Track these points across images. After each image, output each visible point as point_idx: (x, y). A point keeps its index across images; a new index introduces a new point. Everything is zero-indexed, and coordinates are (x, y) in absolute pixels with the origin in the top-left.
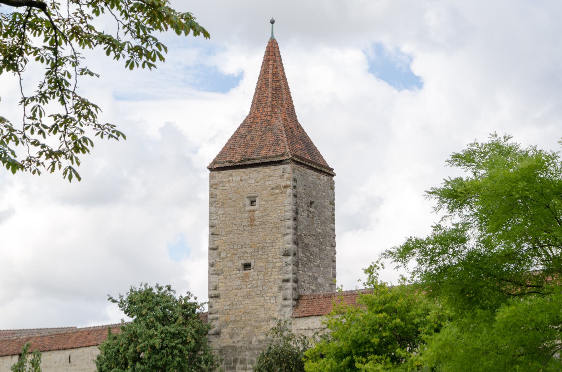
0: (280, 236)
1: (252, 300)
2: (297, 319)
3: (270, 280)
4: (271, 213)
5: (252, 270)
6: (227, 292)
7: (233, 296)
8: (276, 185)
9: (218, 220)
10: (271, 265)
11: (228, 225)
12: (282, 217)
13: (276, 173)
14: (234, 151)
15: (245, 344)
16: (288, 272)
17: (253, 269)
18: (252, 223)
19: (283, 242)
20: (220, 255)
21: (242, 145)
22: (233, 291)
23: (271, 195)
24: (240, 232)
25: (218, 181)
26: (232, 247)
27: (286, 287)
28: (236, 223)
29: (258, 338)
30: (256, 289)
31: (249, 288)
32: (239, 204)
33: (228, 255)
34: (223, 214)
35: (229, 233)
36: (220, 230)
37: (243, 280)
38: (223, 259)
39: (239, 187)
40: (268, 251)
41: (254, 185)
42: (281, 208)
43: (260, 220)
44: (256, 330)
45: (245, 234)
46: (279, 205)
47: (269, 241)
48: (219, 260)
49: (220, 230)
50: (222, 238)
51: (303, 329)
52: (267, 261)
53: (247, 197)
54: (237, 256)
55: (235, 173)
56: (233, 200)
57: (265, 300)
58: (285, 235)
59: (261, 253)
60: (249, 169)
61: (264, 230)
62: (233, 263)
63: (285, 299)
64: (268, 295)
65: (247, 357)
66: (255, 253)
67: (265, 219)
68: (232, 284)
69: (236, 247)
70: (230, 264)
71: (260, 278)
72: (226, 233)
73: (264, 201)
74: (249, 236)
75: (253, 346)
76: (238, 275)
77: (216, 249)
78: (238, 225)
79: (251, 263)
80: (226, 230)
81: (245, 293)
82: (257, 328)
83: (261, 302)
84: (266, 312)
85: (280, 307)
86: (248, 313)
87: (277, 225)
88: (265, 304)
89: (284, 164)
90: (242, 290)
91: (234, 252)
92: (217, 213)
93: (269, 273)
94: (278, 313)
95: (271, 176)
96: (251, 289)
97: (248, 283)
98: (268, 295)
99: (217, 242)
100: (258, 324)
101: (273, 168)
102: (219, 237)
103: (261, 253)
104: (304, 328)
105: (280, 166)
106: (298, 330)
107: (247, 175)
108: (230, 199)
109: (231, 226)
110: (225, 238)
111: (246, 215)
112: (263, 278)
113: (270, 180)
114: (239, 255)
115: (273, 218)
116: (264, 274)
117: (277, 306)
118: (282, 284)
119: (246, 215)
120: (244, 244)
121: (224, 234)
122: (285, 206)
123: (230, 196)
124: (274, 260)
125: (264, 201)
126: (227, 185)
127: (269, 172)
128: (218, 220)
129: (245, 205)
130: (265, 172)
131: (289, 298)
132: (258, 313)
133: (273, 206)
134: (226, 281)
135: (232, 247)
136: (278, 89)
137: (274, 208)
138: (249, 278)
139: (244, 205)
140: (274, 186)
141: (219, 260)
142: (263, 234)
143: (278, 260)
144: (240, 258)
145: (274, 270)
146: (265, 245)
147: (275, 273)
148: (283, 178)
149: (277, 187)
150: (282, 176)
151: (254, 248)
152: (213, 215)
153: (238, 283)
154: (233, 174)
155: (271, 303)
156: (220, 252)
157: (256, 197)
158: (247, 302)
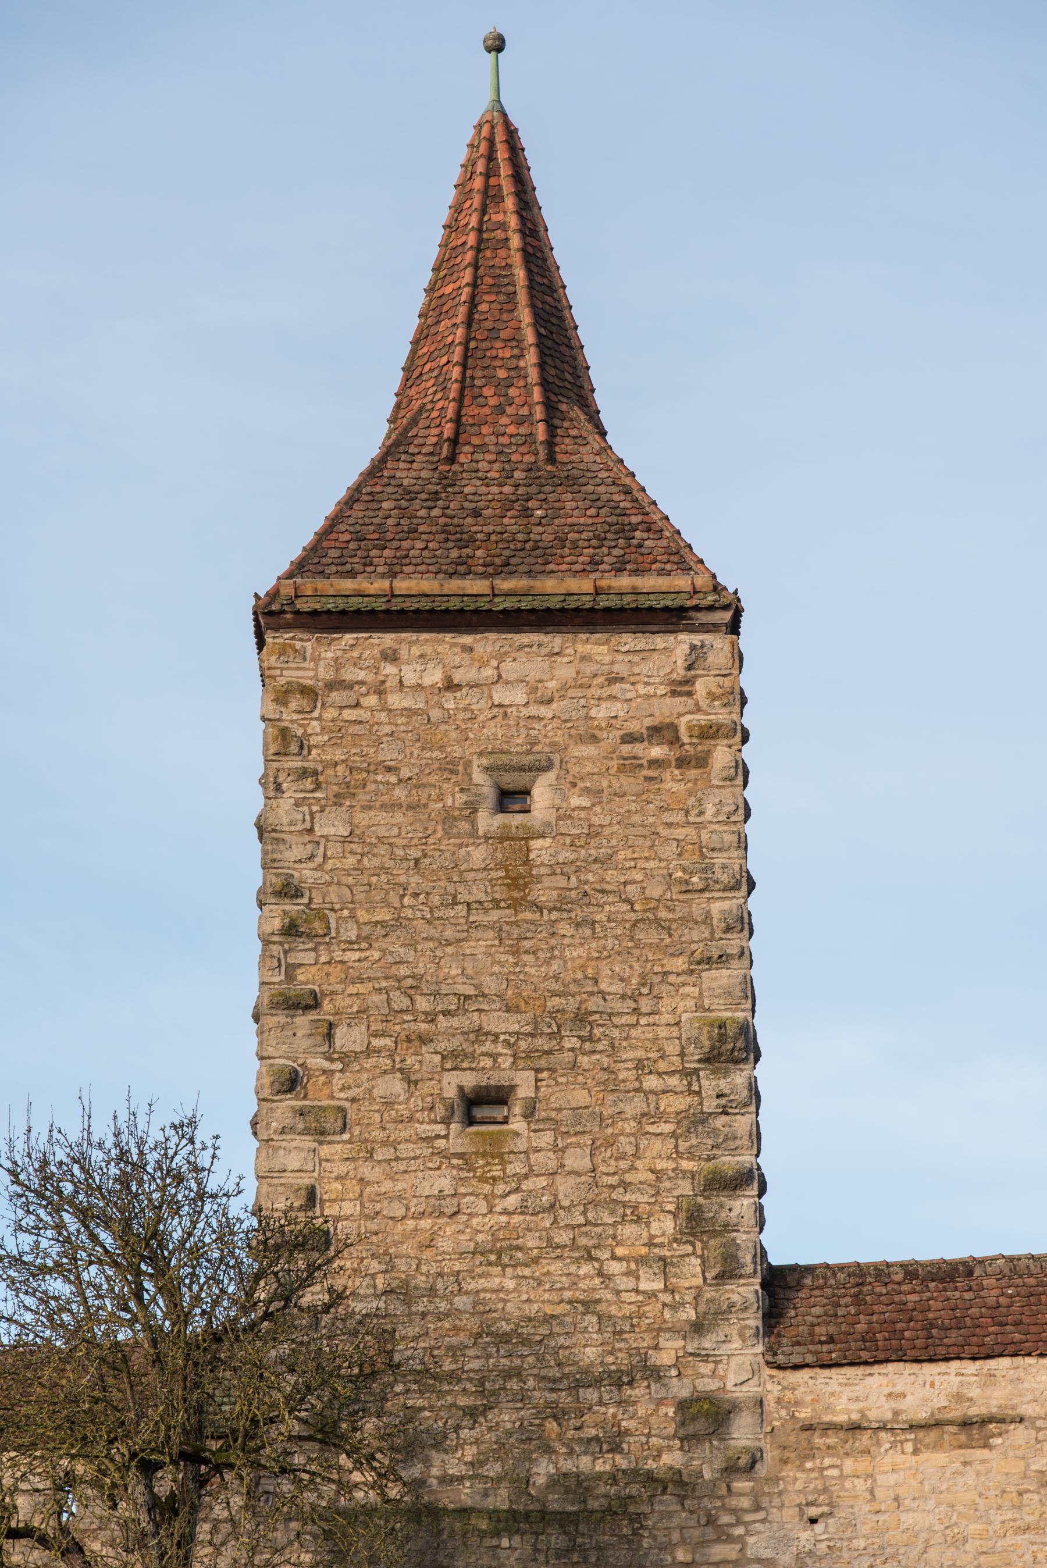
0: (680, 963)
1: (520, 1271)
3: (628, 1177)
7: (408, 1248)
8: (648, 722)
9: (320, 867)
10: (636, 1105)
11: (378, 897)
13: (644, 668)
14: (387, 553)
15: (486, 1494)
16: (732, 1144)
18: (516, 894)
20: (329, 1036)
21: (421, 529)
22: (410, 1224)
23: (622, 769)
25: (315, 677)
26: (400, 1001)
28: (426, 886)
31: (505, 1212)
32: (441, 798)
33: (377, 1043)
34: (344, 840)
35: (379, 931)
38: (347, 1058)
39: (435, 714)
40: (616, 1033)
41: (525, 712)
42: (679, 833)
43: (562, 882)
44: (551, 1426)
45: (480, 944)
46: (667, 817)
47: (617, 988)
48: (326, 1065)
49: (332, 917)
50: (338, 955)
52: (611, 1084)
53: (487, 769)
54: (431, 1047)
55: (416, 651)
56: (405, 773)
57: (600, 1274)
58: (709, 960)
59: (575, 1042)
60: (492, 636)
61: (588, 932)
62: (411, 1083)
64: (620, 1251)
67: (590, 877)
68: (400, 1186)
69: (423, 1004)
70: (395, 1086)
72: (366, 930)
73: (587, 790)
74: (503, 958)
76: (441, 1143)
77: (307, 1008)
78: (436, 900)
79: (512, 1088)
80: (363, 916)
81: (480, 1238)
82: (555, 1417)
86: (504, 1338)
87: (663, 914)
89: (693, 629)
92: (311, 830)
93: (625, 1145)
95: (622, 680)
96: (516, 1219)
97: (500, 1188)
100: (565, 1399)
101: (629, 641)
103: (575, 1042)
105: (671, 638)
108: (389, 769)
109: (394, 899)
110: (356, 955)
111: (478, 855)
113: (612, 697)
114: (442, 1045)
115: (639, 876)
119: (478, 855)
120: (471, 991)
121: (353, 935)
122: (699, 826)
123: (388, 754)
124: (651, 1082)
125: (587, 790)
127: (607, 659)
128: (320, 867)
132: (561, 1340)
133: (637, 819)
134: (366, 1170)
136: (554, 320)
137: (640, 831)
138: (503, 1163)
141: (326, 1065)
143: (674, 1081)
144: (453, 1059)
147: (657, 1145)
148: (690, 694)
150: (682, 683)
151: (529, 1016)
153: (444, 1182)
154: (404, 653)
155: (637, 1291)
156: (331, 1026)
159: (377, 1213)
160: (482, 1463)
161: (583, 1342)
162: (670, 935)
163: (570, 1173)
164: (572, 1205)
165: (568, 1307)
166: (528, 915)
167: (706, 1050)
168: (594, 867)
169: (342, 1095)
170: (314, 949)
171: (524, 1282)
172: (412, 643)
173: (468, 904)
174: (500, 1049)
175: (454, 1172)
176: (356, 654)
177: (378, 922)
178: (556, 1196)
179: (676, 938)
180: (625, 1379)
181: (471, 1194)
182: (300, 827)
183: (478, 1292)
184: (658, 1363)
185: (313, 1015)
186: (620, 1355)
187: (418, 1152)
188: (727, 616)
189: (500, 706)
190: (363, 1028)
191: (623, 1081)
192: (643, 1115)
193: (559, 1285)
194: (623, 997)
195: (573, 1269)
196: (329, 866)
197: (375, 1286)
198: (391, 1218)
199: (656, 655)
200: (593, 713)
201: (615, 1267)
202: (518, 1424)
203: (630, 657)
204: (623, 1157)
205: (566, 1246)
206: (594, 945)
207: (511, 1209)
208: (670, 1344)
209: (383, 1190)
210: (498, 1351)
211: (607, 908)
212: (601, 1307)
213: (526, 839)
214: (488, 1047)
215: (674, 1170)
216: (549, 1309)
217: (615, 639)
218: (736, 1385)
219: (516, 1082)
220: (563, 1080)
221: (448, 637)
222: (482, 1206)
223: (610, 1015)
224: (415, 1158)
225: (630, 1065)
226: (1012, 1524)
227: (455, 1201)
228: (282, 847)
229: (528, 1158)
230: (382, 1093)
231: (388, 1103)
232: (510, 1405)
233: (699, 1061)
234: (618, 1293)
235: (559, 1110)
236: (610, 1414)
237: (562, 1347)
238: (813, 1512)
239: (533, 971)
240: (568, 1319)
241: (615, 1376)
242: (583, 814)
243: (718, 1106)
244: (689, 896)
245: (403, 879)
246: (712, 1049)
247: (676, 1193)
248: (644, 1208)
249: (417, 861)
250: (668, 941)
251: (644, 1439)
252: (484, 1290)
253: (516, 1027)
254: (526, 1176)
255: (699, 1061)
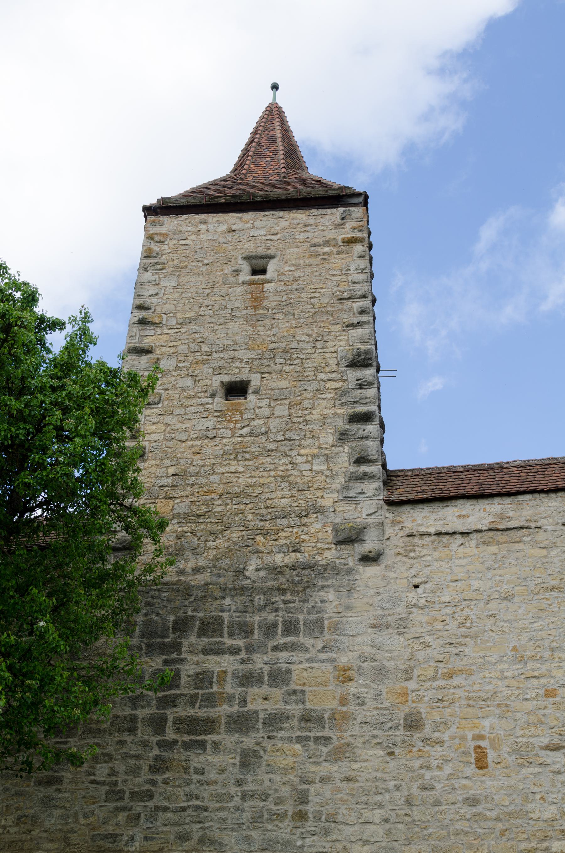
0: (338, 328)
1: (247, 463)
2: (407, 508)
3: (308, 418)
4: (312, 287)
5: (251, 397)
6: (169, 444)
7: (188, 454)
8: (323, 239)
9: (161, 298)
11: (187, 308)
12: (343, 292)
15: (219, 576)
17: (256, 392)
18: (256, 304)
19: (348, 340)
22: (190, 443)
24: (221, 321)
27: (361, 433)
28: (213, 303)
29: (268, 559)
30: (264, 438)
31: (241, 436)
33: (180, 365)
36: (164, 316)
37: (225, 416)
44: (259, 538)
46: (331, 272)
50: (166, 331)
51: (429, 535)
52: (301, 378)
53: (246, 258)
54: (207, 366)
56: (206, 262)
60: (251, 213)
63: (361, 460)
64: (302, 452)
65: (225, 615)
66: (265, 361)
68: (186, 426)
69: (205, 348)
70: (189, 382)
71: (277, 413)
72: (181, 321)
73: (293, 265)
75: (248, 582)
76: (210, 406)
78: (216, 308)
79: (248, 382)
81: (226, 448)
83: (281, 468)
84: (294, 492)
85: (342, 479)
87: (329, 309)
88: (294, 473)
90: (217, 439)
91: (200, 358)
94: (335, 495)
97: (238, 425)
98: (302, 452)
99: (152, 338)
102: (158, 329)
103: (282, 361)
104: (432, 530)
106: (411, 535)
107: (247, 222)
111: (240, 290)
112: (286, 413)
114: (214, 364)
115: (317, 295)
116: (290, 406)
117: (333, 477)
118: (348, 427)
124: (322, 376)
126: (194, 237)
128: (161, 298)
129: (237, 272)
130: (293, 219)
131: (373, 458)
132: (268, 495)
134: (168, 419)
135: (194, 347)
138: (242, 414)
139: (234, 271)
140: (320, 240)
142: (287, 325)
143: (333, 376)
144: (218, 371)
145: (319, 396)
146: (294, 345)
147: (325, 403)
148: (343, 228)
149: (326, 243)
150: (339, 225)
151: (260, 352)
152: (147, 287)
153: (210, 423)
155: (311, 470)
157: (271, 257)
158: (233, 469)
159: (173, 438)
160: (218, 560)
161: (280, 496)
162: (332, 317)
163: (278, 417)
164: (278, 431)
165: (273, 479)
166: (261, 311)
167: (350, 360)
168: (295, 292)
169: (160, 388)
170: (154, 329)
171: (249, 468)
172: (214, 217)
173: (232, 309)
174: (243, 365)
175: (215, 419)
176: (188, 221)
177: (186, 318)
178: (269, 428)
179: (335, 317)
180: (304, 514)
181: (223, 428)
182: (153, 283)
183: (223, 473)
184: (323, 505)
185: (150, 356)
186: (301, 502)
187: (197, 411)
188: (361, 199)
189: (253, 236)
190: (175, 360)
191: (307, 376)
192: (317, 390)
193: (268, 469)
194: (308, 342)
195: (276, 461)
196: (164, 298)
197: (167, 473)
198: (180, 441)
199: (327, 216)
200: (297, 237)
201: (300, 459)
202: (241, 538)
203: (315, 217)
204: (306, 409)
205: (273, 450)
206: (294, 322)
207: (244, 434)
208: (330, 495)
209: (176, 428)
210: (232, 502)
211: (301, 308)
212: (291, 479)
213: (263, 284)
214: (237, 364)
215: (333, 414)
216: (262, 481)
217: (307, 212)
218: (367, 515)
219: (251, 378)
220: (276, 377)
221: (231, 214)
222: (229, 433)
223: (301, 350)
224: (195, 413)
225: (310, 369)
226: (542, 586)
227: (215, 431)
228: (143, 290)
229: (255, 412)
230: (181, 386)
231: (183, 389)
232: (237, 529)
233: (347, 366)
234: (301, 471)
235: (272, 390)
236: (294, 532)
237: (268, 499)
238: (416, 581)
239: (262, 333)
240: (273, 485)
241: (297, 513)
242: (290, 273)
243: (356, 385)
244: (342, 301)
245: (201, 301)
246: (353, 360)
247: (334, 424)
248: (316, 433)
249: (208, 294)
250: (331, 319)
251: (313, 545)
252: (227, 472)
253: (253, 356)
254: (253, 419)
255: (347, 366)
